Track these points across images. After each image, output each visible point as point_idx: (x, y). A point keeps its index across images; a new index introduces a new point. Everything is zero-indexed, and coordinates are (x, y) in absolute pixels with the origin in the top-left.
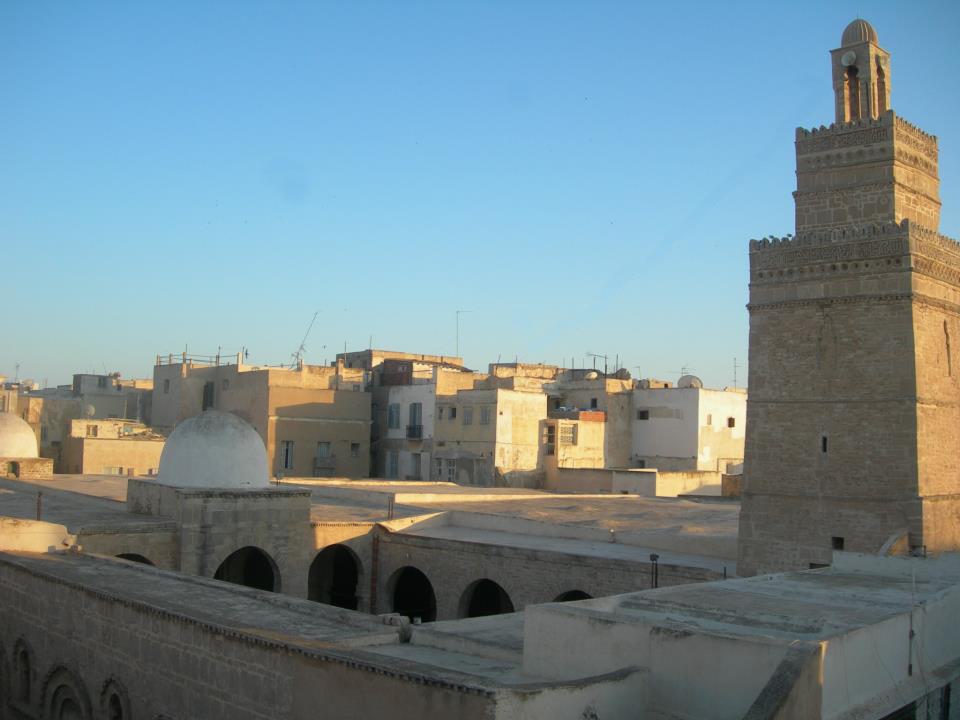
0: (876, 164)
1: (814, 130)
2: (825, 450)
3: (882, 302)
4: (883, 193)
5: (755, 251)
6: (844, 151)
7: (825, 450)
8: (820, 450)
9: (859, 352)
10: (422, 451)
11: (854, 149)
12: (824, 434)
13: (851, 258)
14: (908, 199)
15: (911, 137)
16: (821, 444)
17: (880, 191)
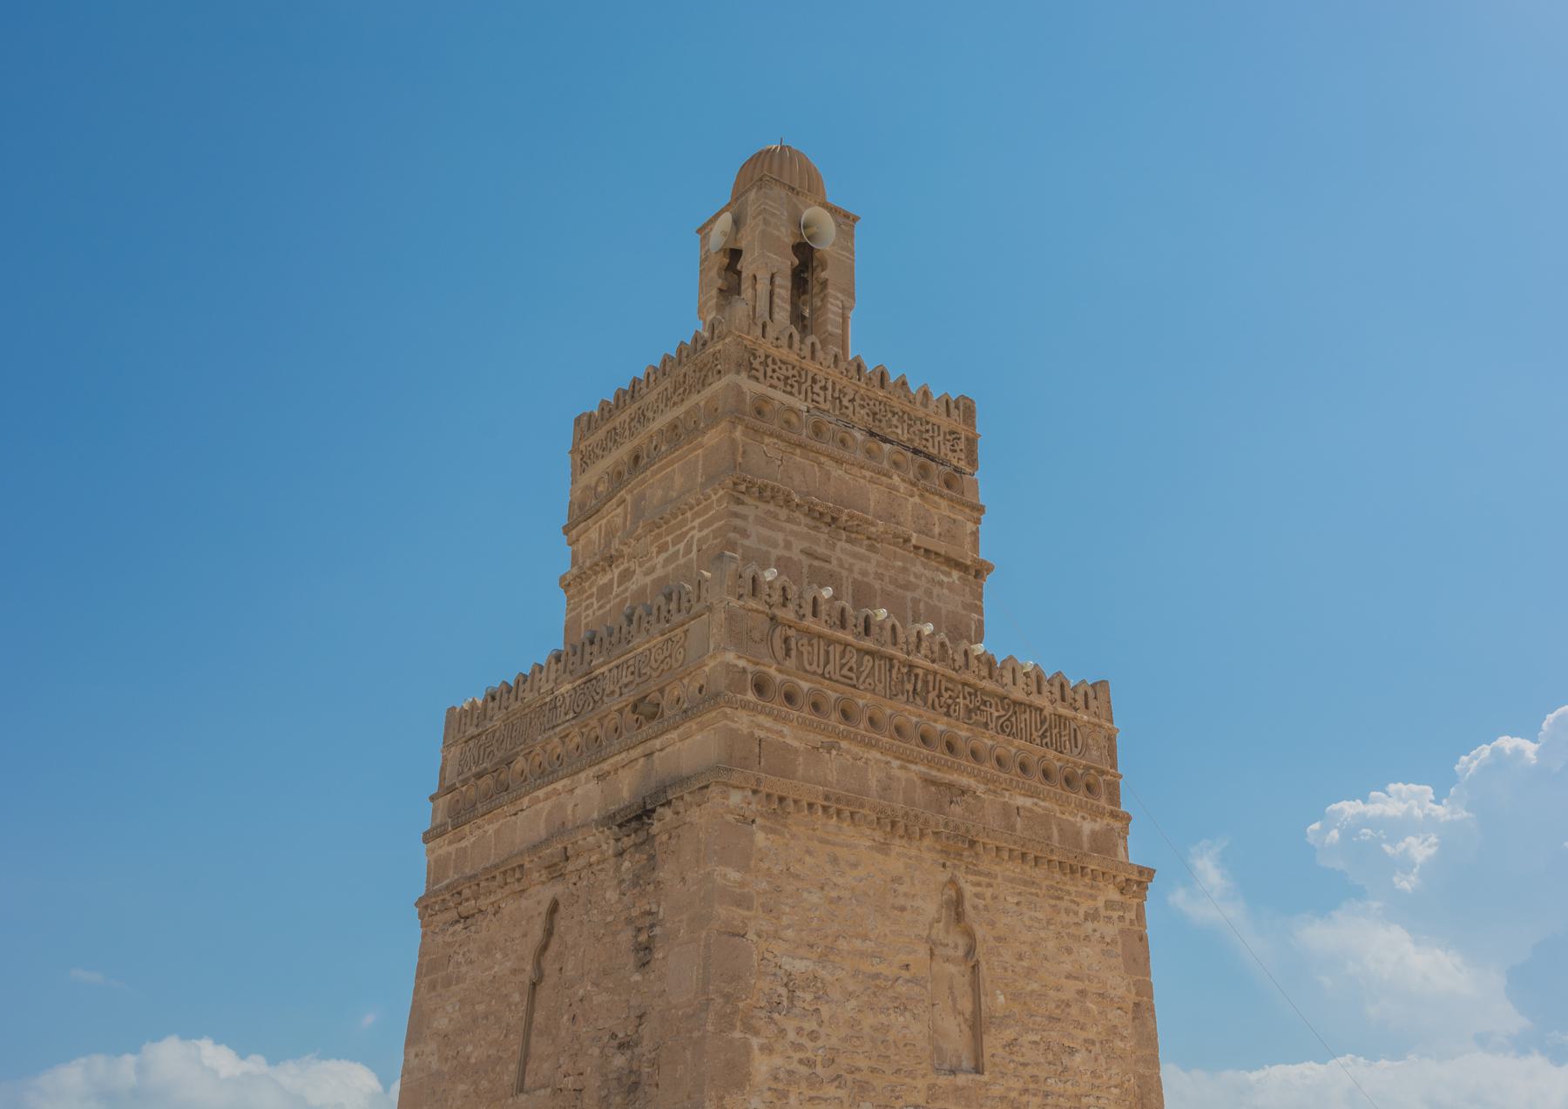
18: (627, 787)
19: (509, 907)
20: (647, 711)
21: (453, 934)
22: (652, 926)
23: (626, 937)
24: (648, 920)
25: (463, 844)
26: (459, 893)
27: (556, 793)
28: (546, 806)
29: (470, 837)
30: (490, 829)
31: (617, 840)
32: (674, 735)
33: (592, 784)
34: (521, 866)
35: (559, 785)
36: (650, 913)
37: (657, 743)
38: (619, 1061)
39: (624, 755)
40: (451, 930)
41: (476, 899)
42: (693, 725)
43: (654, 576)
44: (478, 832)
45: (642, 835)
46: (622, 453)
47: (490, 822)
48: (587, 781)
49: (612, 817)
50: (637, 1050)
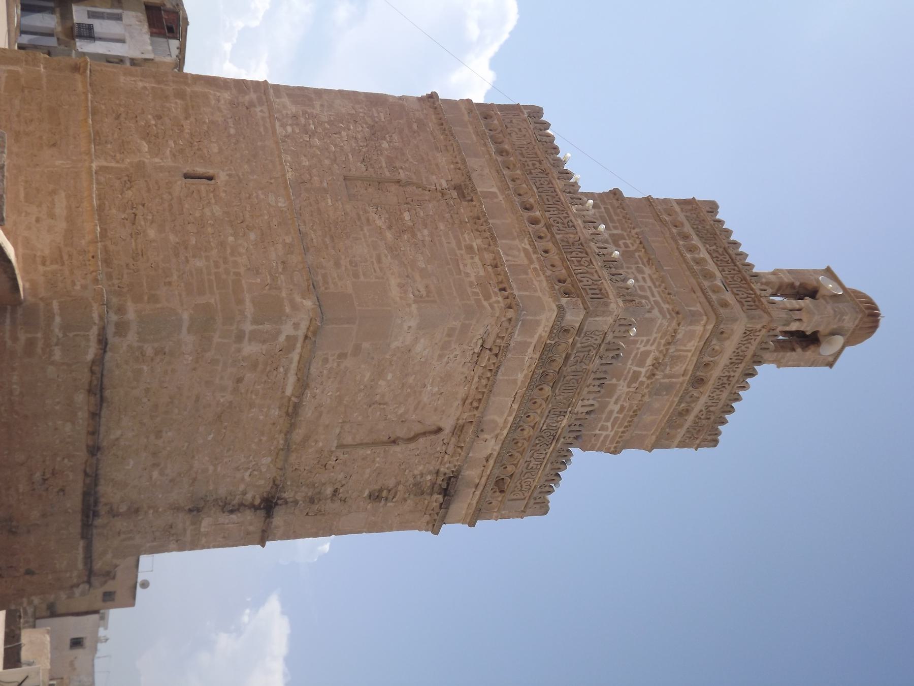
0: (700, 294)
1: (720, 222)
2: (186, 176)
3: (490, 269)
4: (656, 302)
5: (525, 111)
6: (703, 254)
7: (186, 176)
8: (188, 169)
9: (389, 235)
10: (58, 39)
11: (712, 266)
12: (222, 177)
13: (554, 230)
14: (646, 354)
15: (742, 366)
16: (200, 170)
17: (658, 298)
18: (471, 474)
19: (462, 392)
20: (500, 485)
21: (476, 343)
22: (387, 499)
23: (391, 483)
24: (390, 497)
25: (530, 350)
26: (496, 355)
27: (504, 427)
28: (500, 421)
29: (530, 356)
30: (520, 377)
31: (445, 474)
32: (474, 502)
33: (489, 452)
34: (477, 408)
35: (505, 432)
36: (394, 497)
37: (478, 493)
38: (329, 491)
39: (488, 473)
40: (480, 342)
41: (485, 367)
42: (471, 511)
43: (612, 403)
44: (528, 364)
45: (436, 488)
46: (716, 373)
47: (526, 376)
48: (493, 450)
49: (456, 477)
50: (329, 501)
